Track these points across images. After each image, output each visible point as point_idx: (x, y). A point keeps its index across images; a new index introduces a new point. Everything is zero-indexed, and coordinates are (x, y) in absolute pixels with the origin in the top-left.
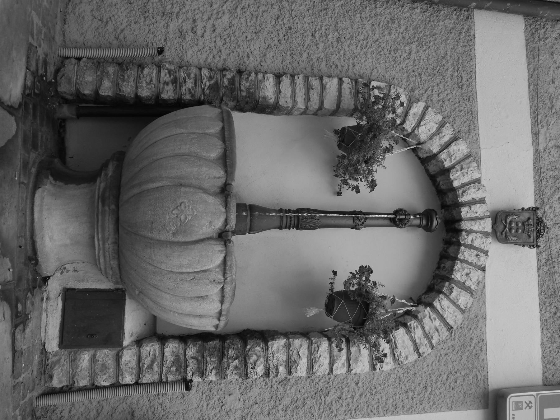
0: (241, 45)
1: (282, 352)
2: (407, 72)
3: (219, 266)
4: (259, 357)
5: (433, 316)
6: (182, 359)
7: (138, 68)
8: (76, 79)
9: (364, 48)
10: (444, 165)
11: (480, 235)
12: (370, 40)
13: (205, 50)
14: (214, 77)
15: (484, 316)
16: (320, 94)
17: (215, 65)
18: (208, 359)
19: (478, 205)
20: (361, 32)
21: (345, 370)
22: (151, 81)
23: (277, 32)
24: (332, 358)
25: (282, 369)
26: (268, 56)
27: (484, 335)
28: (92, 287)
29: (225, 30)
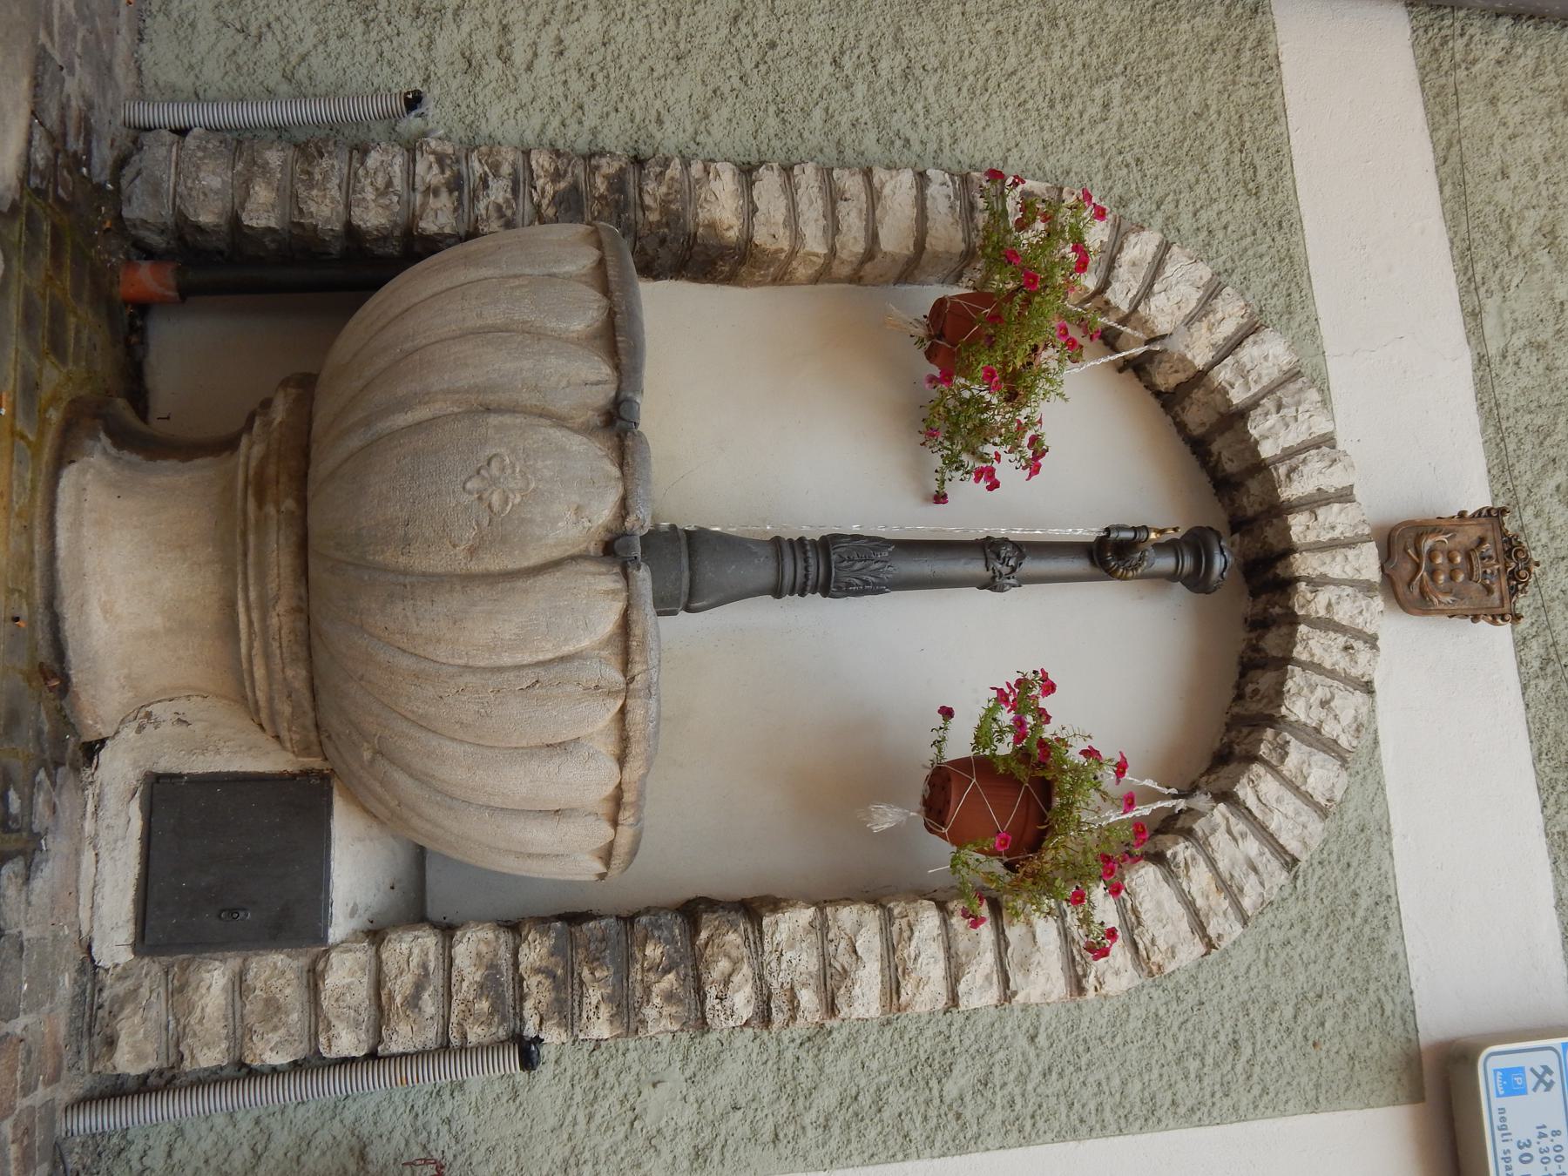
0: (638, 91)
1: (804, 945)
2: (1102, 155)
3: (608, 642)
4: (736, 963)
5: (1239, 826)
6: (506, 977)
7: (351, 153)
8: (176, 184)
9: (978, 92)
10: (1230, 400)
11: (1349, 590)
12: (994, 69)
13: (537, 105)
14: (566, 172)
15: (1385, 828)
16: (867, 215)
17: (569, 144)
18: (586, 973)
19: (1336, 507)
20: (966, 52)
21: (993, 995)
22: (389, 184)
23: (735, 56)
24: (952, 961)
25: (808, 999)
26: (714, 117)
27: (1391, 881)
28: (232, 769)
29: (591, 53)
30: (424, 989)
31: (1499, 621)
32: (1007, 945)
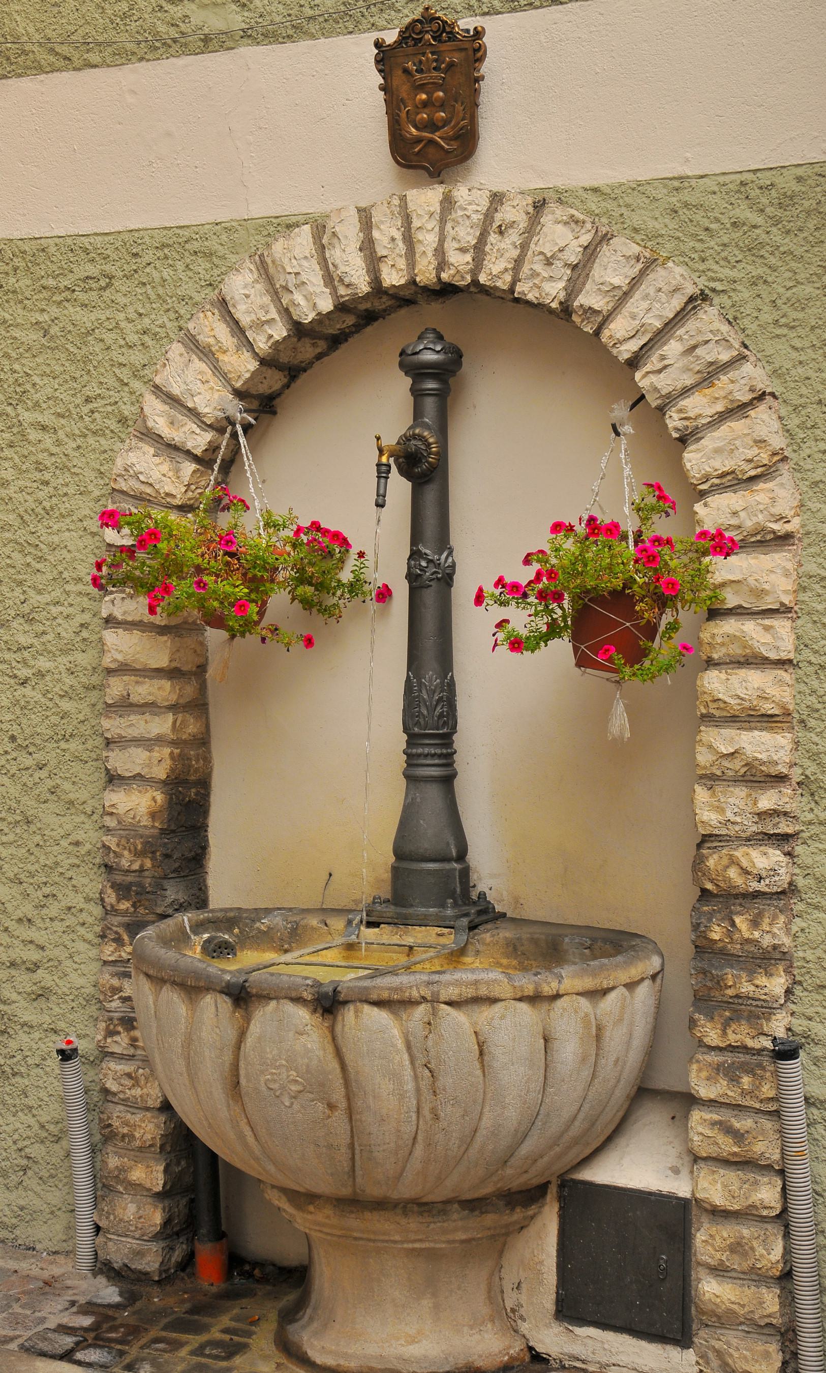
0: (55, 859)
1: (722, 800)
2: (85, 436)
3: (395, 1013)
4: (733, 862)
5: (653, 363)
6: (729, 1058)
7: (108, 1101)
8: (133, 1237)
9: (40, 554)
10: (284, 338)
11: (449, 226)
12: (22, 535)
13: (69, 944)
14: (116, 933)
15: (676, 184)
16: (140, 676)
17: (97, 922)
18: (730, 992)
19: (376, 234)
20: (8, 561)
21: (782, 626)
22: (129, 1075)
23: (23, 772)
24: (750, 660)
25: (767, 800)
26: (72, 796)
27: (727, 179)
28: (555, 1253)
29: (28, 895)
30: (731, 1127)
31: (480, 53)
32: (740, 607)
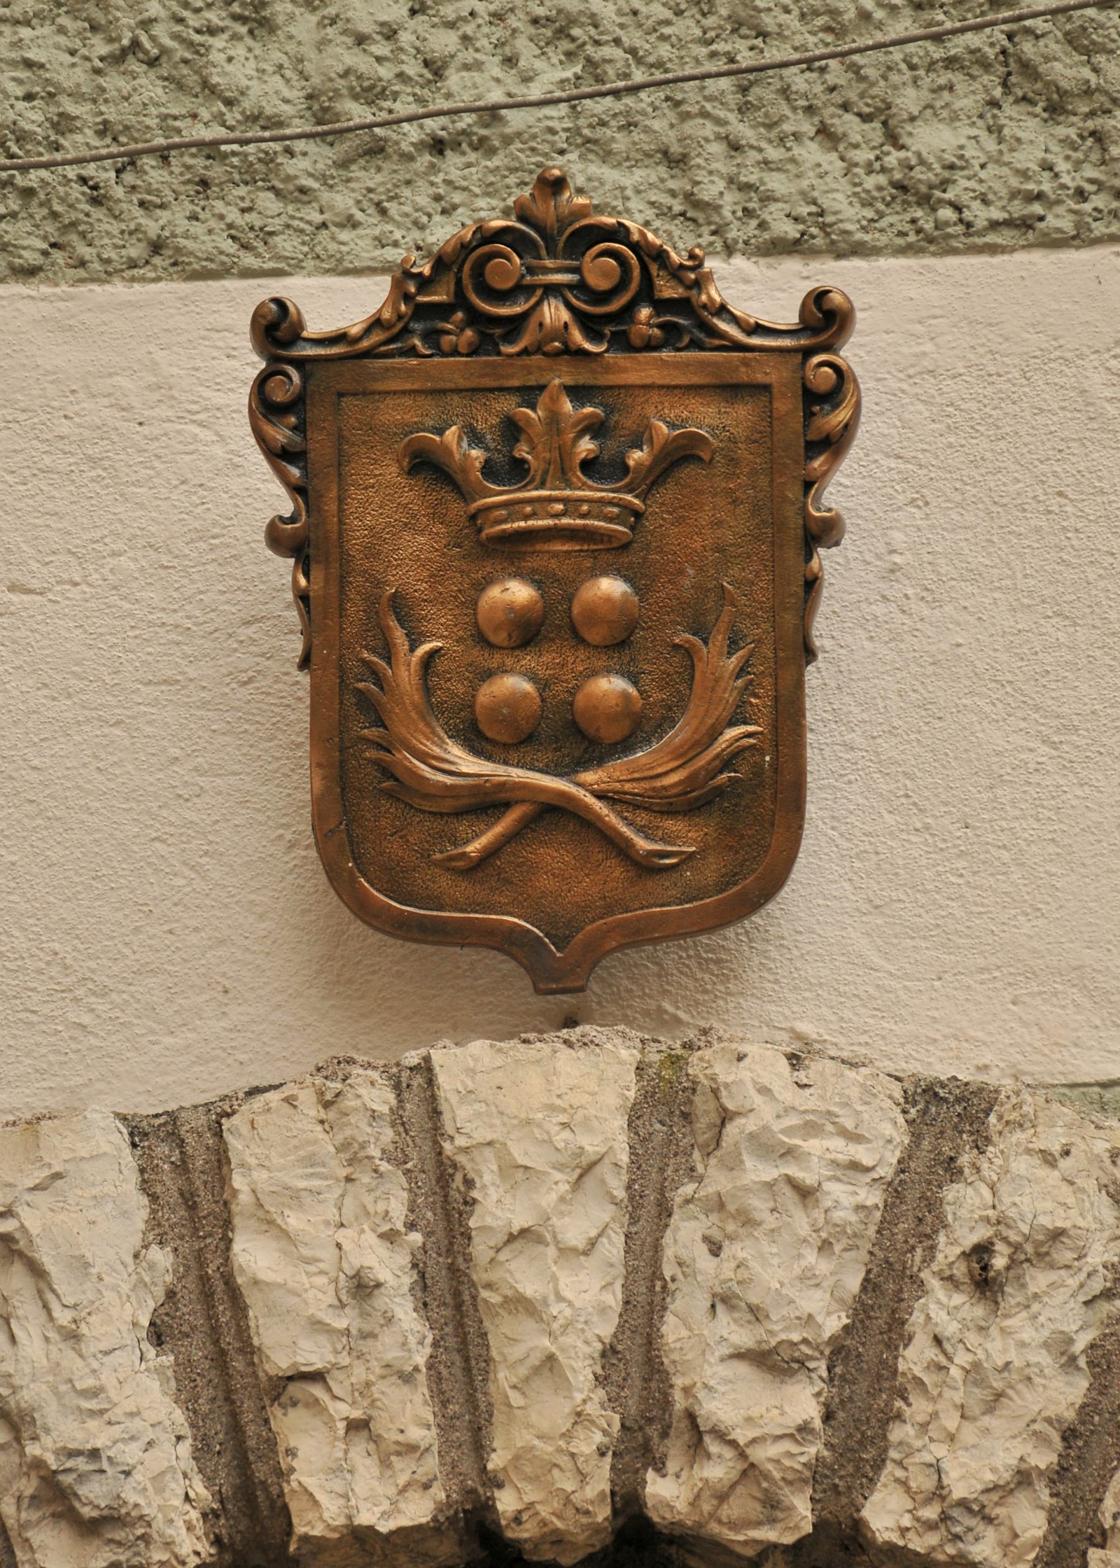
31: (842, 415)
